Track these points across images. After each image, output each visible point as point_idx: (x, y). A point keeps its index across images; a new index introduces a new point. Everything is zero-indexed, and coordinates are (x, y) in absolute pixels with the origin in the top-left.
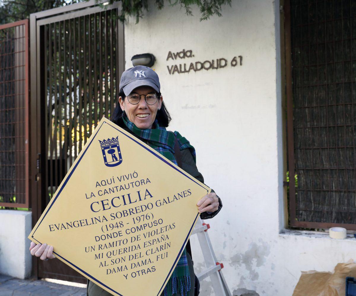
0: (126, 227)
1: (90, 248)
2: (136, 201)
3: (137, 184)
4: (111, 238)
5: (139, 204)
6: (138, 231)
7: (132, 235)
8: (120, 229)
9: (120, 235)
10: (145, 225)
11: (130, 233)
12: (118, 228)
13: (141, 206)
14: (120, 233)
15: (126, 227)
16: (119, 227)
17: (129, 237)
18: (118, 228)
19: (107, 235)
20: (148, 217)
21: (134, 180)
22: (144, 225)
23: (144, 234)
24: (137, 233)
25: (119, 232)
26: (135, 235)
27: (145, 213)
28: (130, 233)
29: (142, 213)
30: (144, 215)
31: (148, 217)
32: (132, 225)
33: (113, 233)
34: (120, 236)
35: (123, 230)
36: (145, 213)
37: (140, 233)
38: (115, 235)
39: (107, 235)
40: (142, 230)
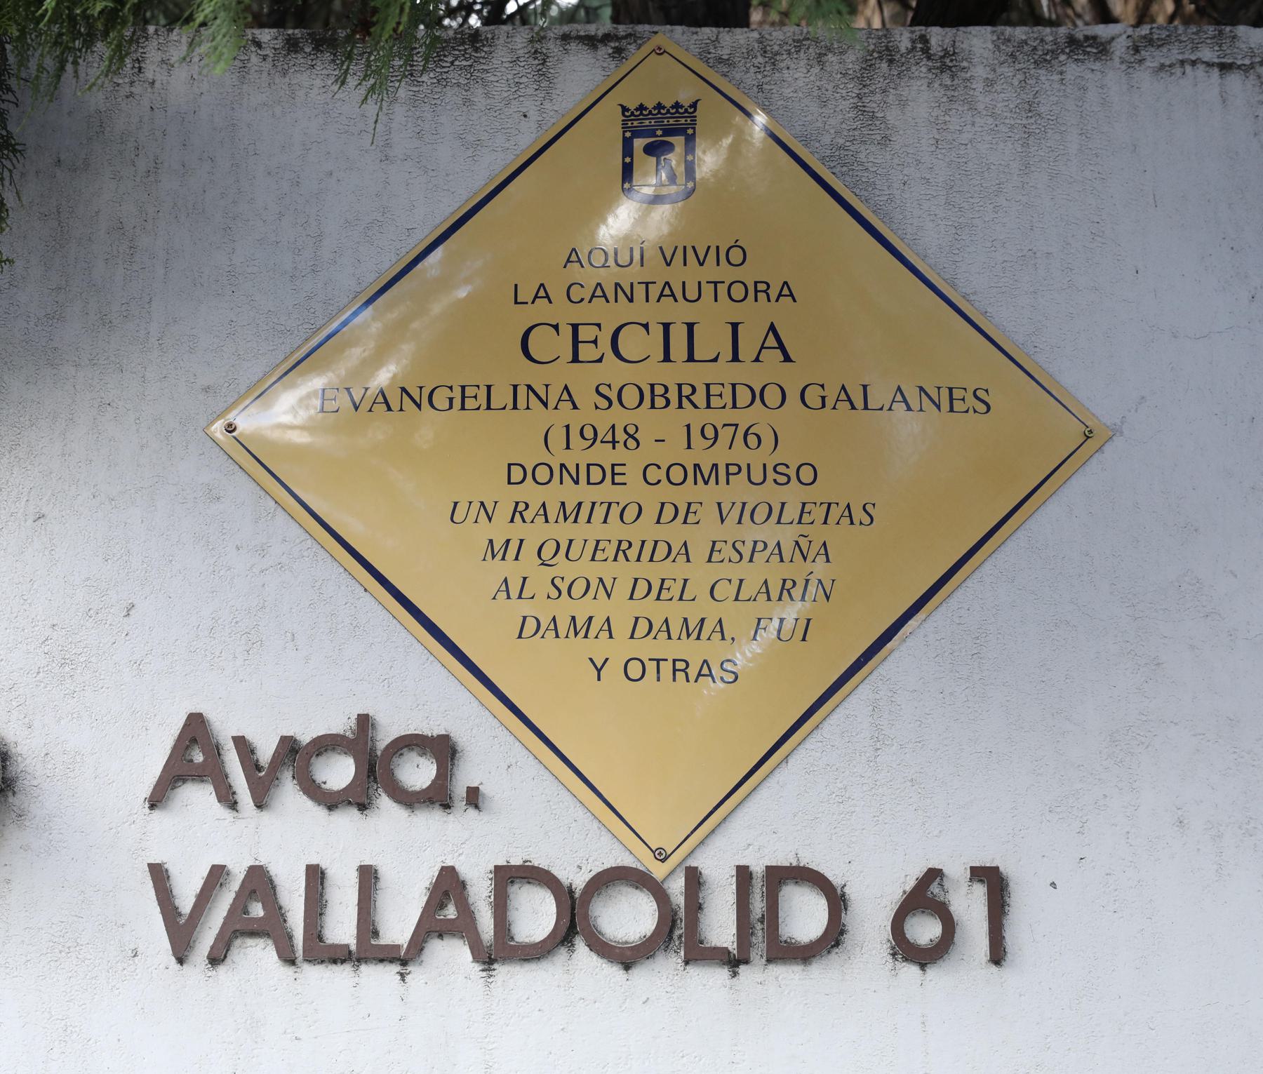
0: (649, 451)
1: (476, 506)
2: (715, 360)
3: (738, 292)
4: (577, 482)
5: (725, 372)
6: (696, 483)
7: (666, 492)
8: (620, 454)
9: (618, 479)
10: (733, 469)
11: (659, 481)
12: (614, 448)
13: (734, 386)
14: (617, 469)
15: (649, 451)
16: (620, 446)
17: (650, 498)
18: (614, 448)
19: (562, 466)
20: (752, 440)
21: (726, 273)
22: (727, 465)
23: (719, 504)
24: (691, 492)
25: (613, 466)
26: (680, 496)
27: (744, 418)
28: (659, 481)
29: (730, 415)
30: (737, 425)
31: (752, 440)
32: (675, 451)
33: (588, 465)
34: (613, 483)
35: (633, 462)
36: (744, 418)
37: (707, 494)
38: (596, 474)
39: (562, 466)
40: (717, 483)
